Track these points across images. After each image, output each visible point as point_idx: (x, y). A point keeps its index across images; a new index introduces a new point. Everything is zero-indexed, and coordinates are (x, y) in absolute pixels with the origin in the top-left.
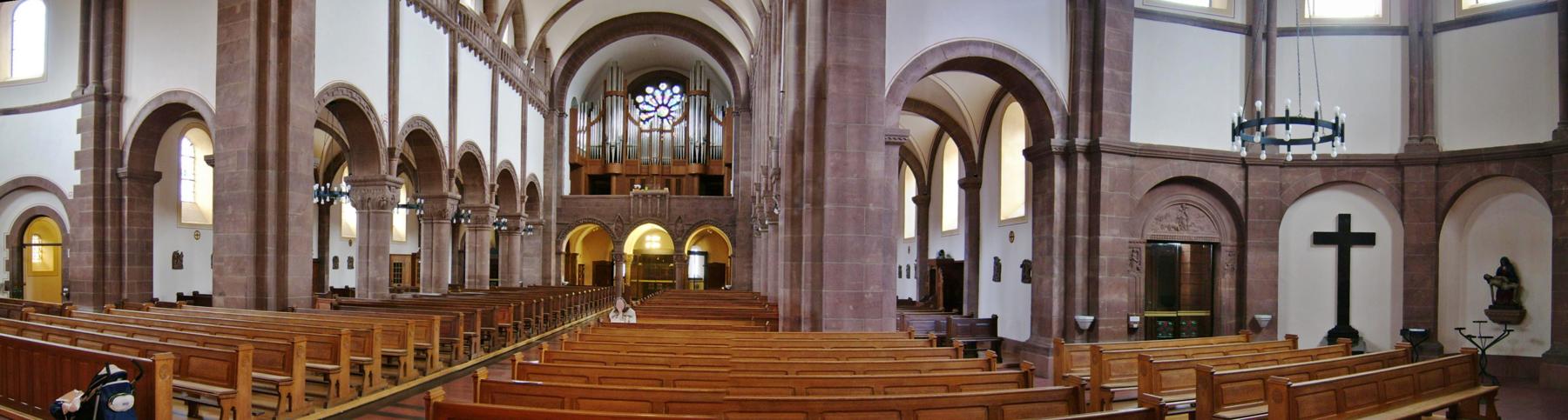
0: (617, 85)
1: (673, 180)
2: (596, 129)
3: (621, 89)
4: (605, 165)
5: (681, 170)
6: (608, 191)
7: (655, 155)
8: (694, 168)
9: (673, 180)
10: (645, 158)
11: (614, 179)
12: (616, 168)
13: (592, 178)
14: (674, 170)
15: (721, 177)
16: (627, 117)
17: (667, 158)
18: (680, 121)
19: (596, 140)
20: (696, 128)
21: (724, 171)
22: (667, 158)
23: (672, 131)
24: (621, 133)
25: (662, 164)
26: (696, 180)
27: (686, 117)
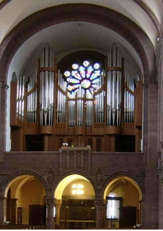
0: (49, 63)
1: (94, 140)
2: (31, 98)
3: (52, 66)
4: (39, 128)
5: (101, 131)
6: (42, 149)
7: (79, 119)
8: (111, 130)
9: (94, 140)
10: (72, 121)
11: (46, 138)
12: (48, 130)
13: (28, 138)
14: (95, 131)
15: (133, 138)
16: (57, 88)
17: (89, 121)
18: (99, 92)
19: (31, 106)
20: (112, 98)
21: (135, 132)
22: (89, 121)
23: (93, 100)
24: (52, 102)
25: (85, 126)
26: (113, 139)
27: (104, 88)
